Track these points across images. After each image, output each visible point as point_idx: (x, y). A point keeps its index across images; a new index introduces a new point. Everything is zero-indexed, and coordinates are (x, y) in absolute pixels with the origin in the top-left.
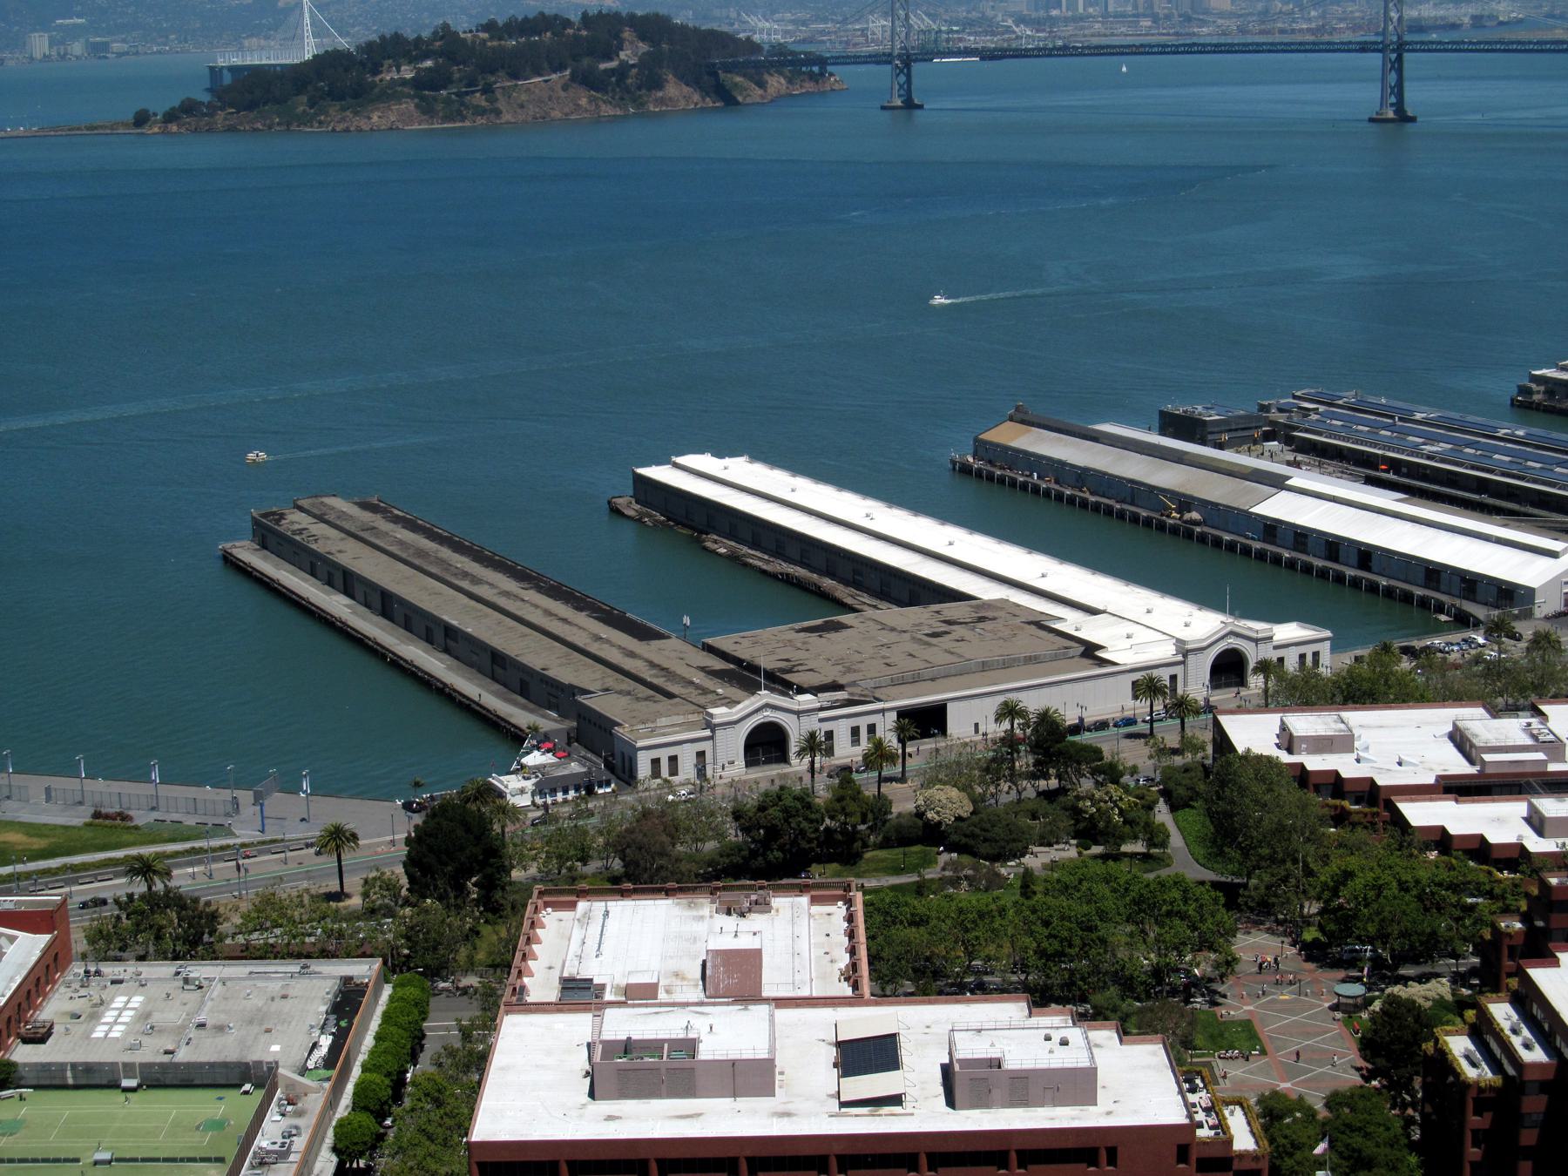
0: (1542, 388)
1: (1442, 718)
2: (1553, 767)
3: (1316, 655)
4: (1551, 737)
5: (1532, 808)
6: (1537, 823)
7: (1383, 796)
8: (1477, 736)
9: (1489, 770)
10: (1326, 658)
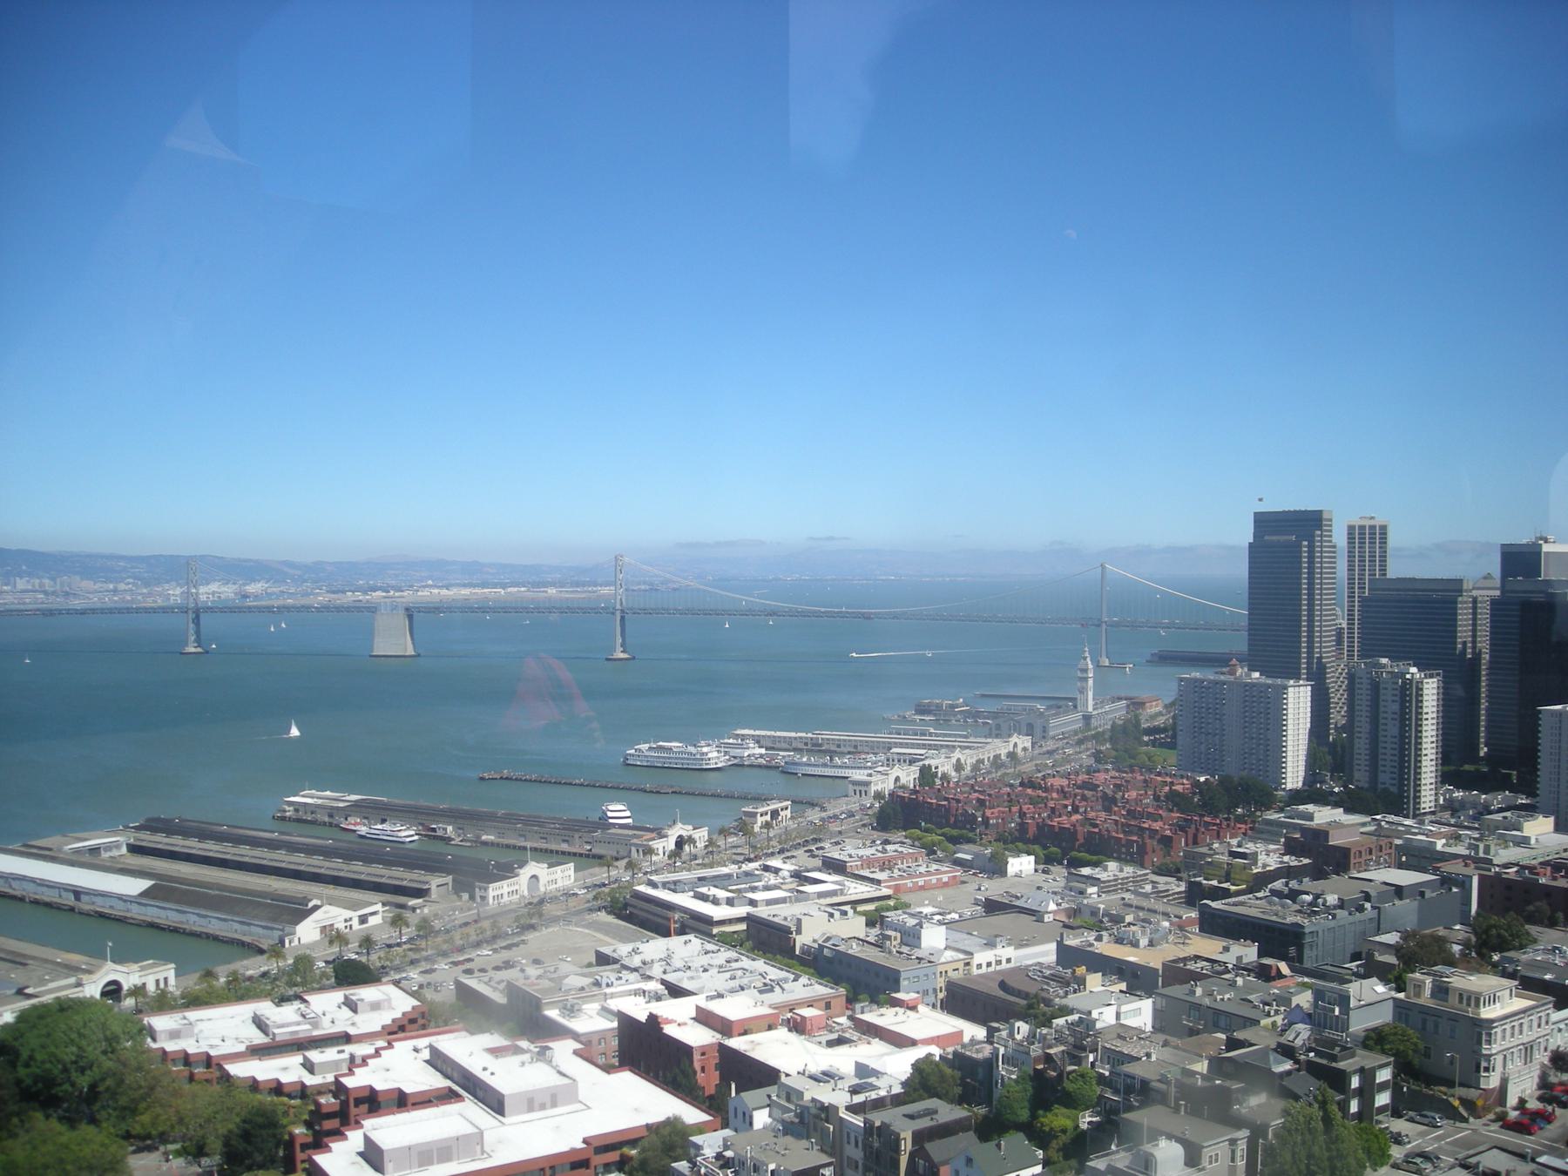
0: (291, 808)
1: (245, 1010)
2: (316, 1033)
3: (166, 979)
4: (313, 1015)
5: (305, 1058)
6: (309, 1067)
7: (214, 1062)
8: (268, 1019)
9: (277, 1039)
10: (172, 981)
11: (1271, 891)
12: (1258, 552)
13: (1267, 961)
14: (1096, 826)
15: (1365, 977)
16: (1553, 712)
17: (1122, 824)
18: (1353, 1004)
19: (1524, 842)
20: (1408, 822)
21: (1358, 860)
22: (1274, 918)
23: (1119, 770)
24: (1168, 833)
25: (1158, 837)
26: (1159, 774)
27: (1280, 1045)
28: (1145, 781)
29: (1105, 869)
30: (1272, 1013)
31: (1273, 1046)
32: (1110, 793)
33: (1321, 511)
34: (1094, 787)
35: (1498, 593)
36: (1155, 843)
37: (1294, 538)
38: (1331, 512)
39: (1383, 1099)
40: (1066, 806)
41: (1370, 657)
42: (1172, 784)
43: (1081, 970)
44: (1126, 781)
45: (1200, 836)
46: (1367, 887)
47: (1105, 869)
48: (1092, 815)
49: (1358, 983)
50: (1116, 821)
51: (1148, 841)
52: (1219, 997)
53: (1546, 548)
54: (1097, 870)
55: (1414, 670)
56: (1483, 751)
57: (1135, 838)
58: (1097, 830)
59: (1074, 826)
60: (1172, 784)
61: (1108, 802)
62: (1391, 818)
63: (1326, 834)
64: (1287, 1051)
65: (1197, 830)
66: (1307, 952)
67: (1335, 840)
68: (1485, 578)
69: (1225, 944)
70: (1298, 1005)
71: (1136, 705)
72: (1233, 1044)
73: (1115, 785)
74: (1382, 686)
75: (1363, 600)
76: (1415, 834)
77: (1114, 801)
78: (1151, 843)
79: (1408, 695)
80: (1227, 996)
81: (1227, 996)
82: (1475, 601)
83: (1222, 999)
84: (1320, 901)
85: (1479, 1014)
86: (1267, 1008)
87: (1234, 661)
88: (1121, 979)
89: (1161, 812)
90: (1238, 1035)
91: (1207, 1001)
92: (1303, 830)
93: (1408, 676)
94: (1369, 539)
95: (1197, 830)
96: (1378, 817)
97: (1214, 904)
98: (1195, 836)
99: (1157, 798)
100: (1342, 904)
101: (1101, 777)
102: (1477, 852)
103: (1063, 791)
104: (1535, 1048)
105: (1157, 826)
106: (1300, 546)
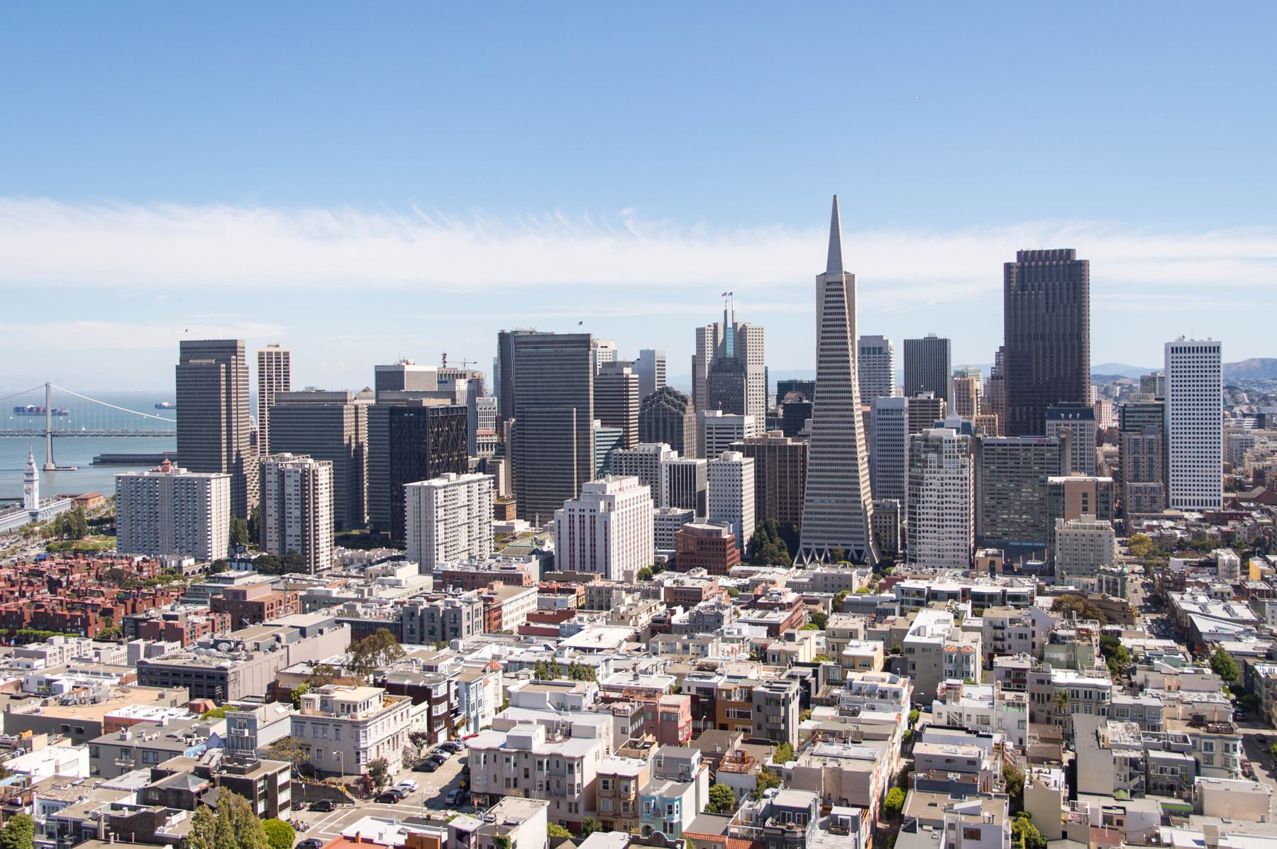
11: (199, 643)
12: (182, 372)
13: (197, 701)
14: (43, 606)
15: (268, 702)
16: (414, 487)
17: (67, 603)
18: (259, 724)
19: (397, 584)
20: (309, 577)
21: (270, 611)
22: (202, 665)
23: (65, 558)
24: (109, 606)
25: (100, 610)
26: (101, 558)
27: (197, 769)
28: (88, 564)
29: (51, 643)
30: (194, 743)
31: (192, 770)
32: (55, 577)
33: (236, 341)
34: (40, 574)
35: (373, 402)
36: (97, 616)
37: (214, 361)
38: (243, 341)
39: (284, 797)
40: (12, 593)
41: (277, 452)
42: (112, 564)
43: (27, 735)
44: (71, 566)
45: (138, 605)
46: (275, 630)
47: (51, 643)
48: (39, 597)
49: (263, 708)
50: (61, 601)
51: (91, 614)
52: (147, 738)
53: (407, 368)
54: (43, 645)
55: (311, 461)
56: (367, 518)
57: (79, 613)
58: (42, 610)
59: (21, 608)
60: (112, 564)
61: (54, 586)
62: (298, 575)
63: (244, 593)
64: (203, 773)
65: (135, 601)
66: (230, 687)
67: (251, 598)
68: (365, 391)
69: (160, 692)
70: (214, 734)
71: (80, 500)
72: (157, 775)
73: (61, 571)
74: (286, 474)
75: (270, 409)
76: (316, 586)
77: (59, 583)
78: (93, 616)
79: (306, 481)
80: (154, 736)
81: (154, 736)
82: (356, 408)
83: (151, 739)
84: (240, 647)
85: (356, 717)
86: (189, 740)
87: (167, 461)
88: (66, 736)
89: (102, 589)
90: (161, 767)
91: (136, 743)
92: (226, 592)
93: (307, 466)
94: (275, 364)
95: (135, 601)
96: (287, 576)
97: (150, 661)
98: (134, 606)
99: (99, 578)
100: (257, 647)
101: (47, 564)
102: (363, 596)
103: (10, 579)
104: (400, 737)
105: (98, 601)
106: (219, 368)
